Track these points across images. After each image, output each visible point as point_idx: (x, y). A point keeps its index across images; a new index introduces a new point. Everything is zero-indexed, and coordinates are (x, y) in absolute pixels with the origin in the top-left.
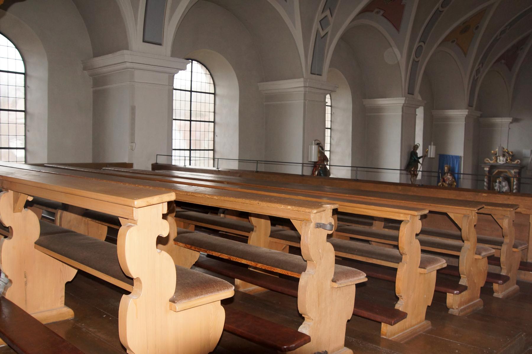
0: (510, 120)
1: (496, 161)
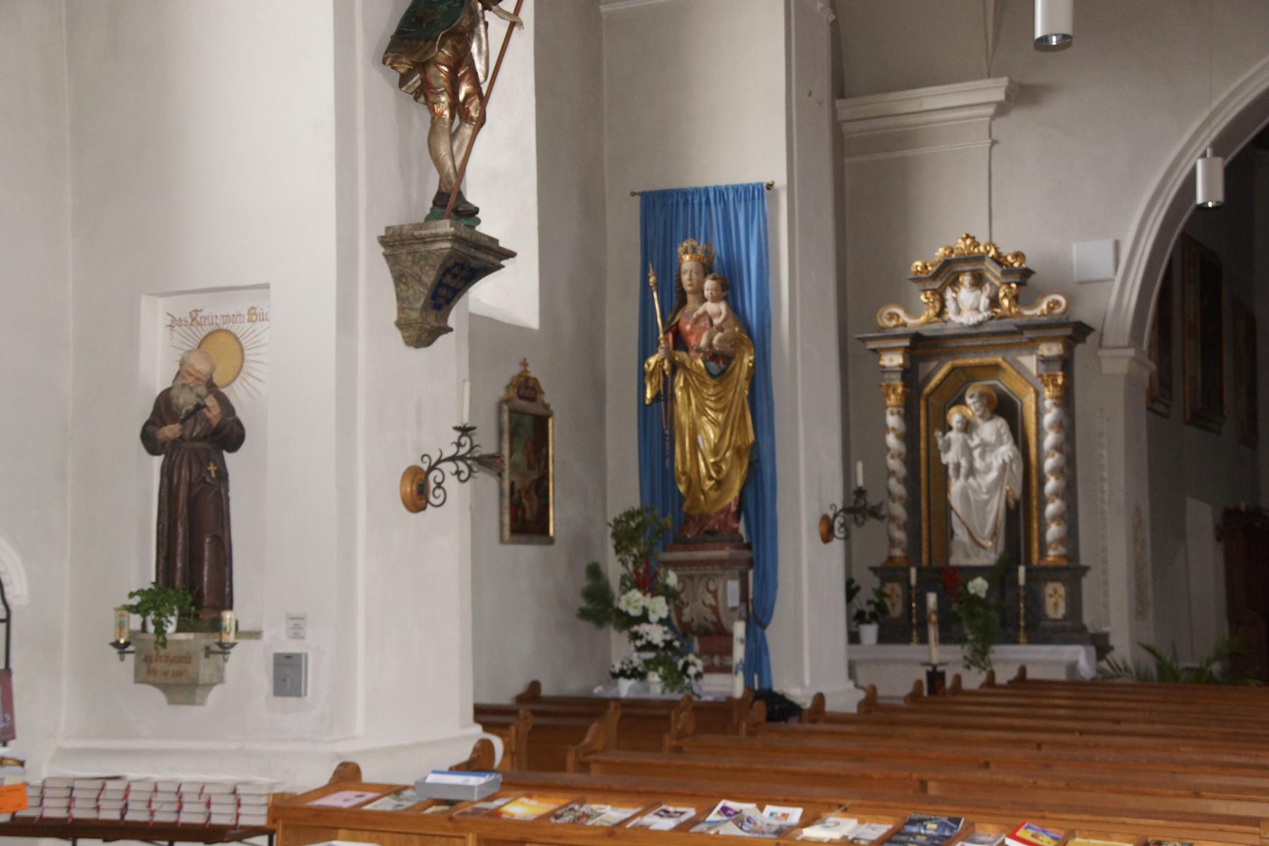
0: (995, 90)
1: (941, 313)
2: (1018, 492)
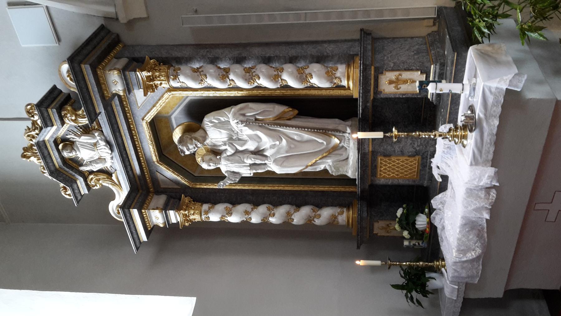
2: (279, 109)
